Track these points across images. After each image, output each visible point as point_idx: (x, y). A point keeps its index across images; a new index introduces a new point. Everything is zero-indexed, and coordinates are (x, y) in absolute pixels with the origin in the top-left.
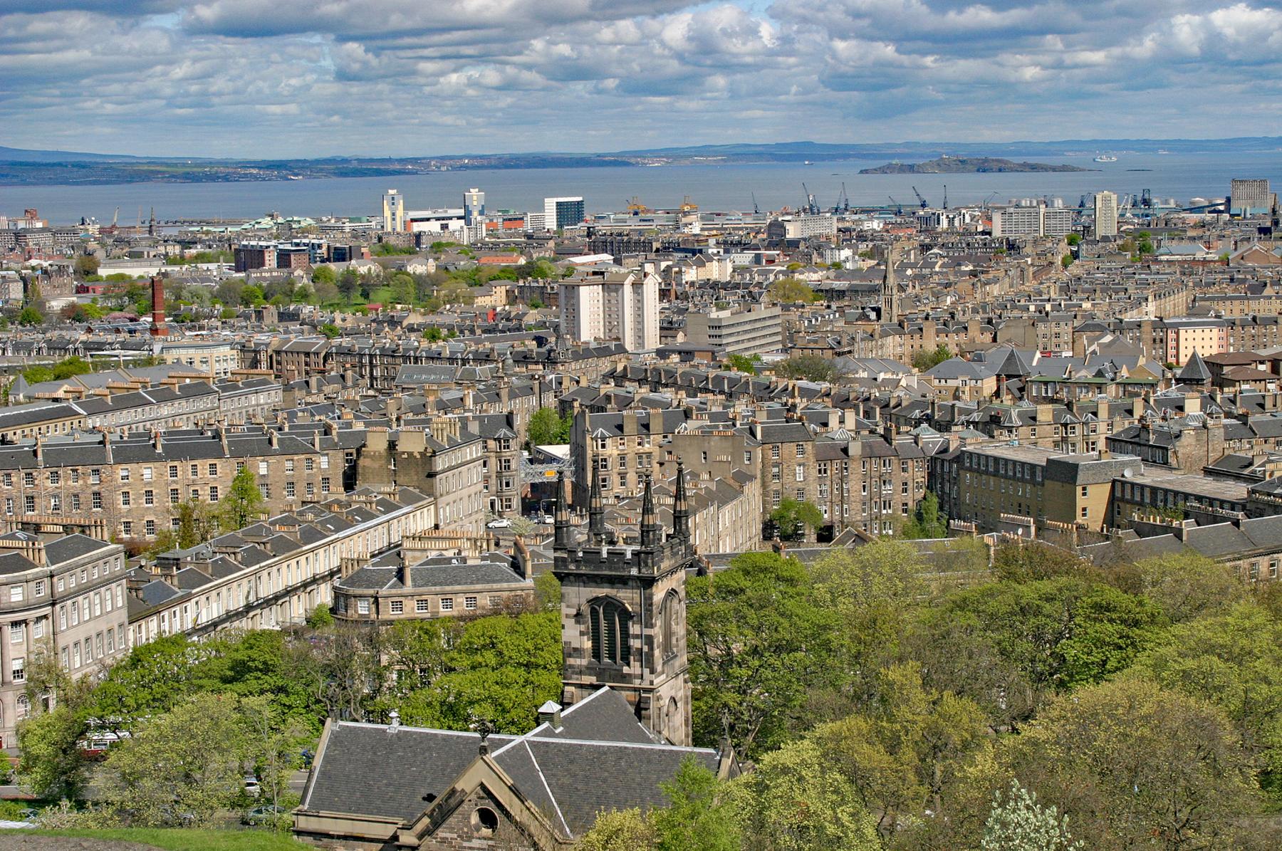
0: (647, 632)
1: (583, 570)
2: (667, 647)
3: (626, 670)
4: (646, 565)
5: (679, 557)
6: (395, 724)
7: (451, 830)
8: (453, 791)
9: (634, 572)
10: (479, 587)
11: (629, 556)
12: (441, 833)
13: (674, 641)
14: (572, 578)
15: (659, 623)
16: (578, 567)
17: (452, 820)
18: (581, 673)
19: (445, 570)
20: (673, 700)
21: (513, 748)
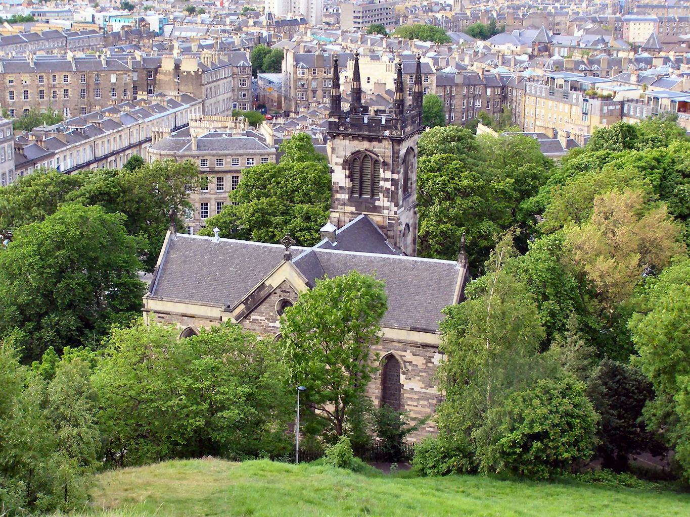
0: (396, 176)
1: (350, 131)
2: (405, 189)
3: (377, 203)
4: (396, 129)
5: (416, 125)
6: (216, 237)
7: (261, 314)
10: (241, 152)
11: (383, 122)
12: (253, 316)
13: (409, 185)
14: (341, 137)
15: (402, 171)
16: (346, 129)
17: (262, 308)
18: (344, 204)
19: (219, 141)
20: (407, 225)
21: (306, 256)
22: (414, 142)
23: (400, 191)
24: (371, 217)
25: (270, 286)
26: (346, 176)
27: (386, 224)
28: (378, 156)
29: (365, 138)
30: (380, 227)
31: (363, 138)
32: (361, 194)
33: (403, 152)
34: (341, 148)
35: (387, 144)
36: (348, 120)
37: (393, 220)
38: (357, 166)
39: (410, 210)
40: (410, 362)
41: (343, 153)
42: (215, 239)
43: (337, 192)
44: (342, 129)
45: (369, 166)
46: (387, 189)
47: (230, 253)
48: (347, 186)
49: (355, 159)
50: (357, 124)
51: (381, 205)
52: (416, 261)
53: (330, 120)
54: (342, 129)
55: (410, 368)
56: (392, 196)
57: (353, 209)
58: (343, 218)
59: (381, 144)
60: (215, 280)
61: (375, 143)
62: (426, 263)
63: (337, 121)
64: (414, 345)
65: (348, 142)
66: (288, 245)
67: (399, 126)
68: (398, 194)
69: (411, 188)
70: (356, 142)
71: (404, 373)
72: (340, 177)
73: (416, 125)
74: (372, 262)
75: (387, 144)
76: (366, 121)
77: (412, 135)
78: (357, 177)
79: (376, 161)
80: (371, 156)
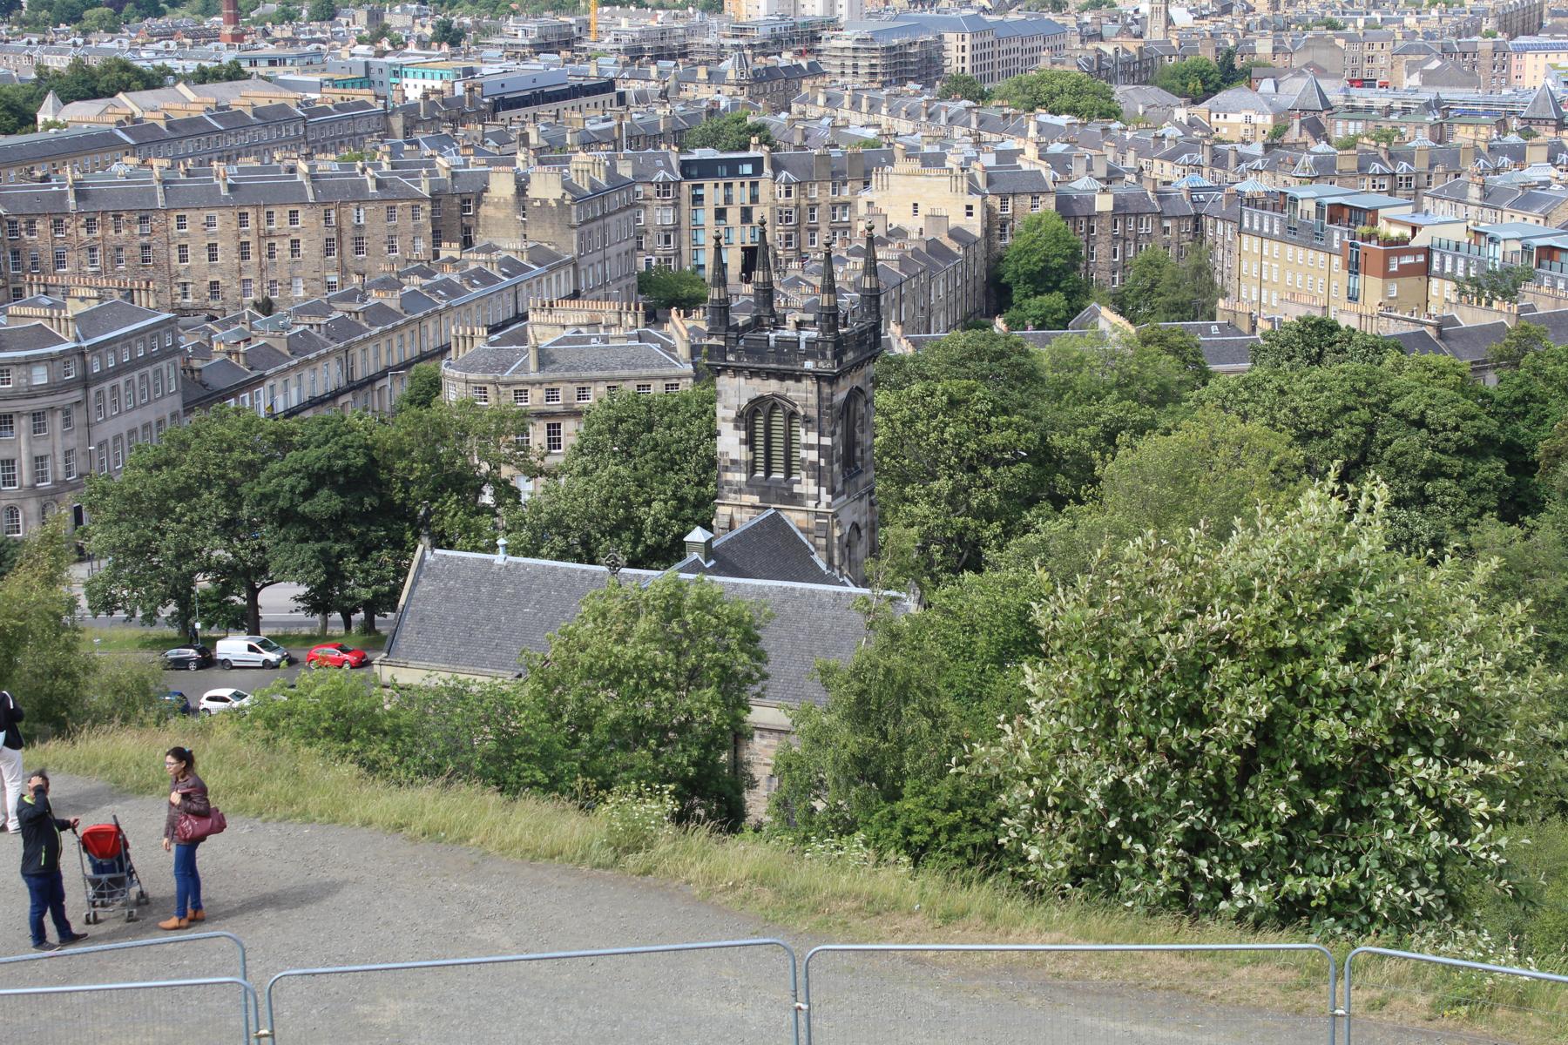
1: (745, 362)
3: (797, 489)
4: (824, 357)
5: (866, 347)
9: (809, 365)
10: (625, 373)
13: (858, 453)
16: (738, 358)
18: (739, 491)
19: (581, 351)
20: (856, 527)
23: (836, 467)
26: (742, 442)
27: (812, 525)
29: (769, 374)
30: (803, 531)
32: (768, 472)
33: (841, 396)
34: (731, 392)
35: (808, 385)
36: (742, 342)
38: (760, 422)
39: (861, 497)
41: (734, 401)
42: (499, 558)
43: (727, 469)
44: (731, 358)
45: (779, 420)
46: (812, 463)
54: (731, 358)
56: (818, 474)
57: (755, 500)
58: (737, 516)
60: (498, 629)
61: (790, 383)
65: (742, 380)
66: (614, 567)
67: (829, 353)
69: (862, 459)
70: (756, 381)
72: (730, 443)
74: (766, 595)
75: (808, 385)
79: (792, 415)
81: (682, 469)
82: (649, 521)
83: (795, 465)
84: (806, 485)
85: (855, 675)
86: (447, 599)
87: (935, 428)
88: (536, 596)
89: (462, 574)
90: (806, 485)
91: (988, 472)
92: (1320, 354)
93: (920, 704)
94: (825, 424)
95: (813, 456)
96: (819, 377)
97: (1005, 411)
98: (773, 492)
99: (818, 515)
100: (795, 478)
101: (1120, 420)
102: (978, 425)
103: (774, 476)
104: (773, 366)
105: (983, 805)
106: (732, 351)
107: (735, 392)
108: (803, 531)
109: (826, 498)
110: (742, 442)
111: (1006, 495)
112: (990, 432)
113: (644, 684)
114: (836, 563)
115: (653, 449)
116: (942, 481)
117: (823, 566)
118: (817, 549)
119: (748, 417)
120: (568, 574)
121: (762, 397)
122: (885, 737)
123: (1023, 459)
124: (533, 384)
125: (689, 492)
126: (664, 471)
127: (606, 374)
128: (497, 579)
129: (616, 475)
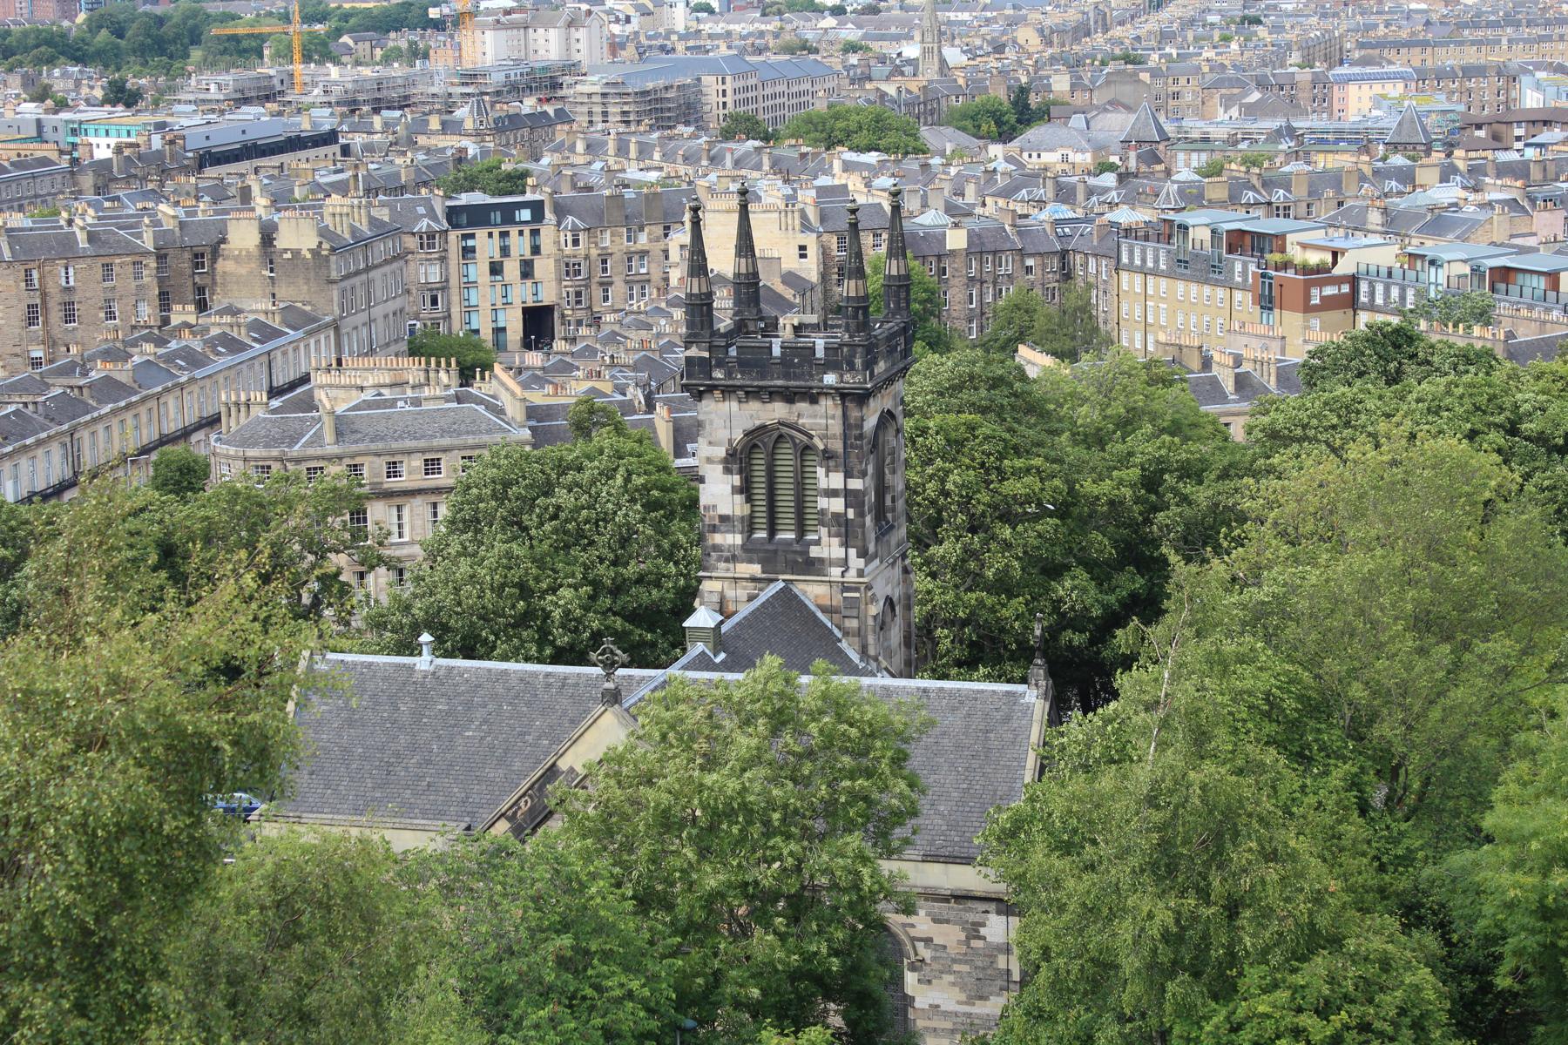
1: (739, 379)
2: (880, 512)
3: (814, 552)
4: (852, 367)
5: (897, 355)
8: (552, 772)
9: (830, 379)
10: (446, 441)
11: (820, 353)
13: (888, 502)
14: (717, 394)
15: (870, 469)
16: (729, 375)
18: (733, 559)
19: (389, 417)
20: (889, 602)
22: (895, 397)
23: (868, 519)
24: (801, 586)
25: (572, 770)
26: (735, 490)
27: (838, 600)
28: (811, 437)
29: (773, 394)
31: (771, 393)
32: (772, 531)
33: (871, 422)
34: (719, 422)
35: (828, 405)
36: (733, 352)
37: (857, 590)
39: (893, 564)
40: (928, 941)
41: (723, 435)
42: (424, 662)
43: (714, 529)
44: (718, 374)
45: (786, 460)
46: (836, 515)
47: (463, 693)
48: (738, 512)
49: (755, 446)
50: (756, 362)
51: (825, 555)
52: (925, 691)
53: (689, 353)
54: (718, 374)
55: (925, 953)
56: (846, 531)
57: (756, 569)
58: (730, 594)
59: (816, 407)
60: (428, 762)
61: (803, 406)
62: (951, 694)
63: (706, 355)
64: (933, 896)
65: (734, 405)
66: (610, 666)
67: (858, 362)
68: (864, 525)
69: (893, 510)
70: (754, 406)
71: (913, 968)
72: (719, 493)
73: (897, 355)
75: (828, 405)
76: (776, 351)
77: (890, 380)
78: (760, 491)
79: (806, 450)
80: (792, 438)
81: (591, 543)
82: (557, 614)
83: (811, 519)
84: (828, 547)
85: (1152, 801)
86: (350, 723)
87: (931, 477)
88: (480, 714)
89: (370, 686)
90: (828, 547)
91: (1007, 532)
92: (1399, 371)
93: (1259, 840)
94: (853, 460)
95: (837, 505)
96: (843, 395)
97: (1018, 454)
98: (781, 558)
99: (845, 588)
100: (811, 537)
101: (1159, 461)
102: (987, 472)
103: (780, 536)
104: (780, 382)
105: (1371, 1001)
106: (720, 365)
107: (727, 420)
108: (824, 610)
109: (856, 563)
110: (735, 490)
111: (1029, 559)
112: (1004, 479)
113: (756, 830)
114: (872, 652)
115: (555, 517)
116: (946, 544)
117: (855, 657)
118: (846, 633)
119: (739, 459)
120: (524, 679)
121: (763, 427)
122: (1204, 895)
123: (1051, 514)
124: (329, 459)
125: (605, 572)
126: (567, 547)
127: (422, 444)
128: (423, 690)
129: (509, 555)
